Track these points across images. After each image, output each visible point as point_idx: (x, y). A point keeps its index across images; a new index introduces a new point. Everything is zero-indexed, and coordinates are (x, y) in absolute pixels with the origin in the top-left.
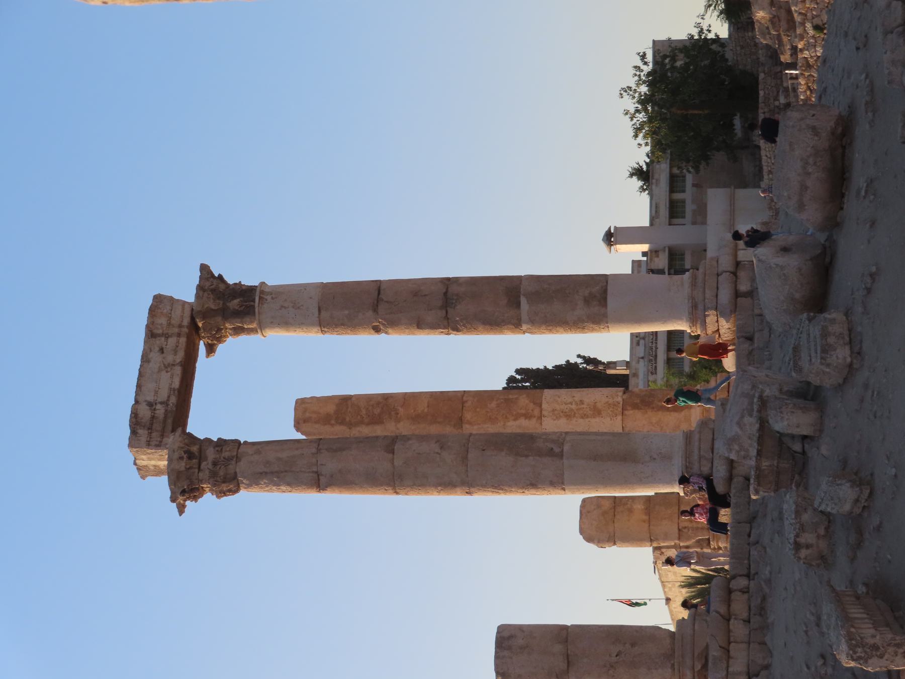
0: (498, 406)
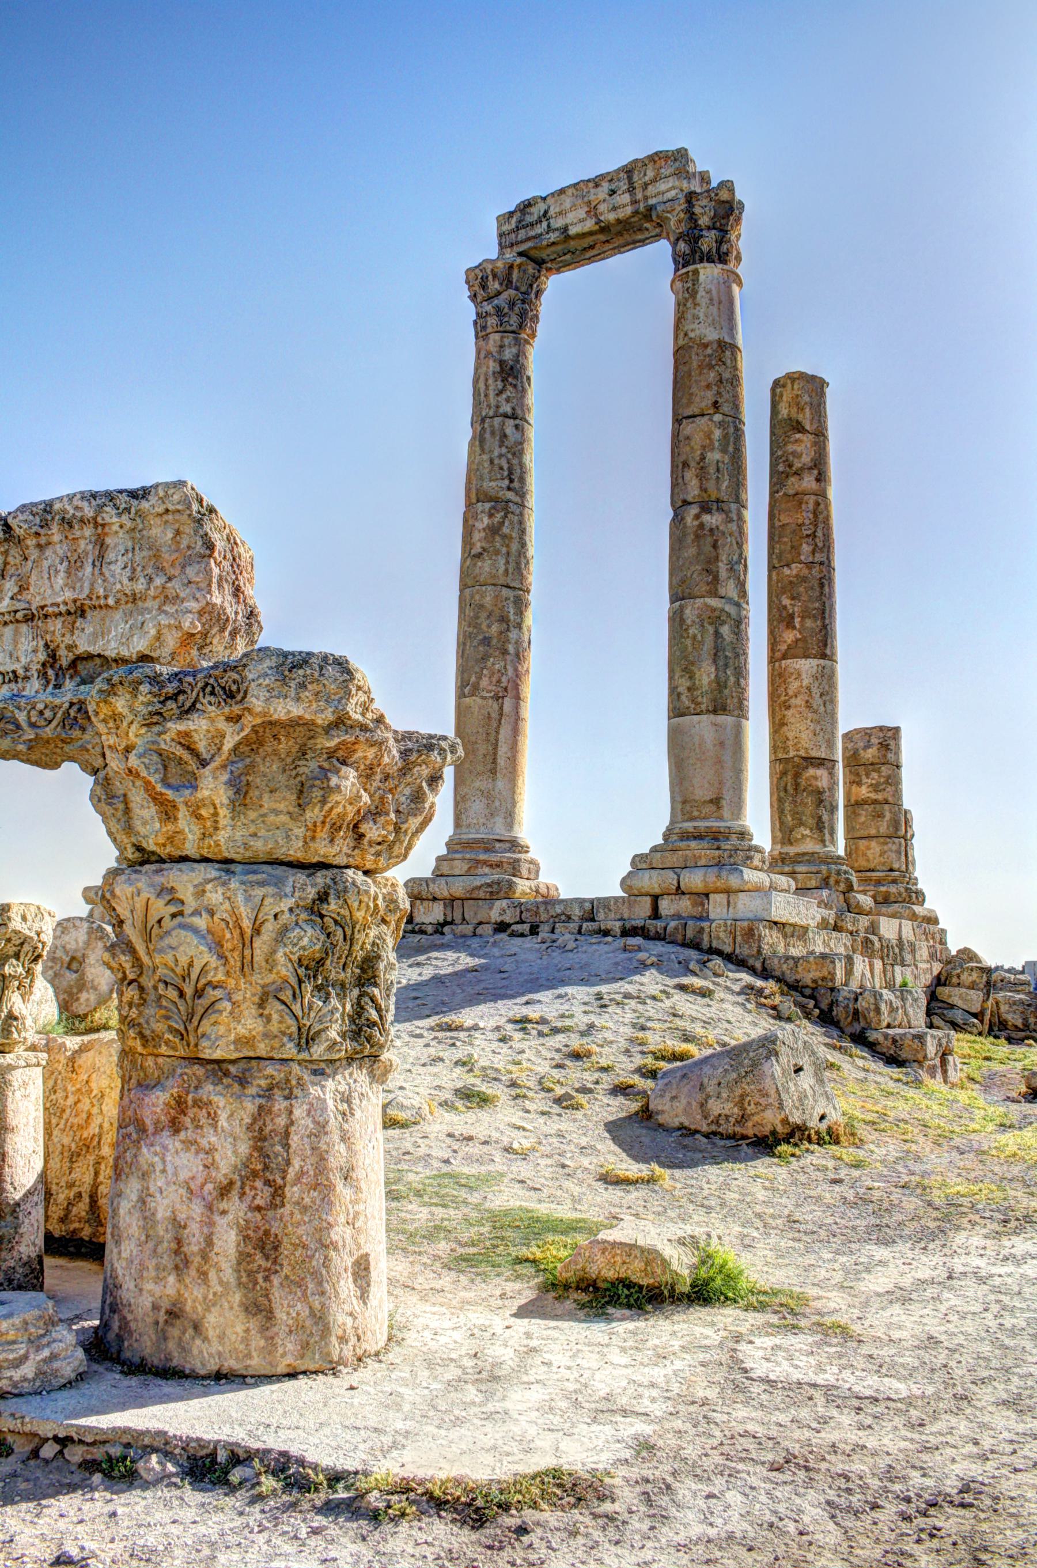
0: (785, 607)
